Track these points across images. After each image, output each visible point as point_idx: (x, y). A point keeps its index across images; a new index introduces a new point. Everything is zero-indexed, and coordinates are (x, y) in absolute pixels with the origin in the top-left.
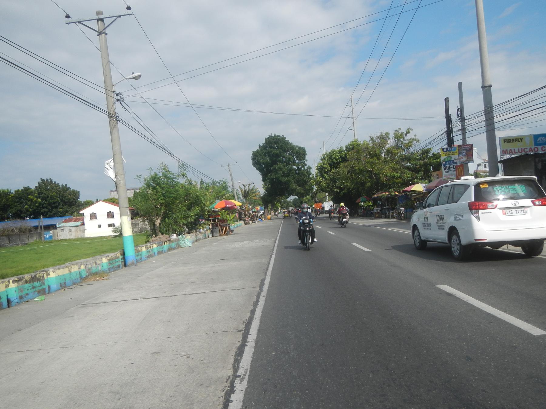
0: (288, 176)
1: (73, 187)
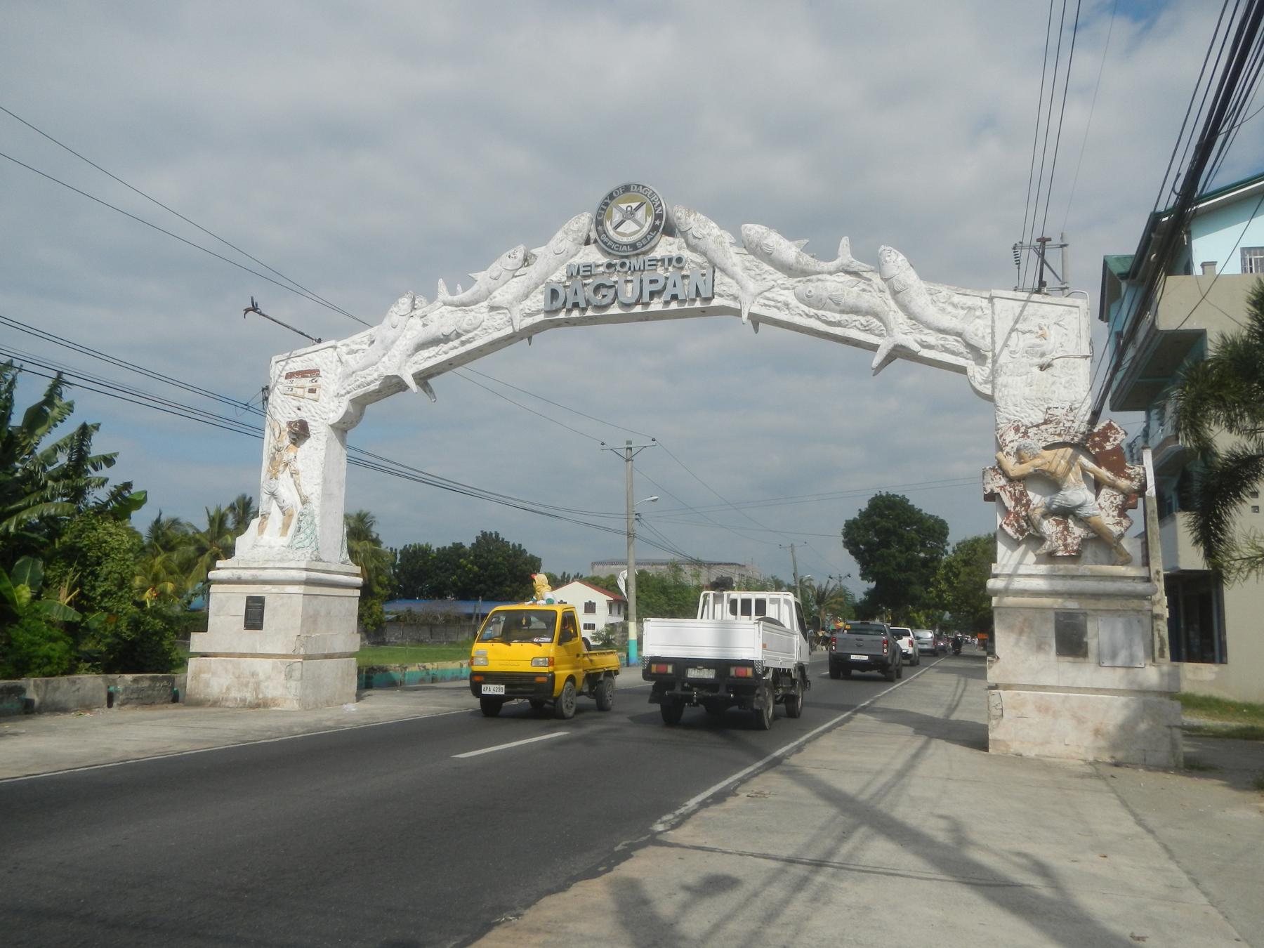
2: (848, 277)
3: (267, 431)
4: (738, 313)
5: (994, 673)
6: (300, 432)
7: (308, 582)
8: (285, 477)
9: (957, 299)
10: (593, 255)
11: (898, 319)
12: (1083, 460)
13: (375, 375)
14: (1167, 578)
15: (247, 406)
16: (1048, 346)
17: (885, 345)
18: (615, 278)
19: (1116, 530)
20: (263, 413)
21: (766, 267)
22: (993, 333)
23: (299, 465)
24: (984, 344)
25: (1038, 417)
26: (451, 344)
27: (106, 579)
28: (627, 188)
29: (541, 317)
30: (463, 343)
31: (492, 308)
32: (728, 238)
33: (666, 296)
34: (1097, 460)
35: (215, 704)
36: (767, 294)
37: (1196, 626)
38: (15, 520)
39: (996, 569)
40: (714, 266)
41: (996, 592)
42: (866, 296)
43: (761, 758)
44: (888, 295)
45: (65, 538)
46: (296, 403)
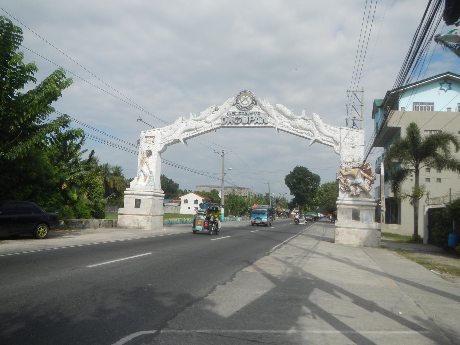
0: (306, 193)
1: (175, 181)
2: (304, 121)
3: (140, 153)
4: (275, 128)
5: (337, 224)
6: (149, 153)
7: (154, 195)
8: (145, 165)
9: (332, 128)
10: (235, 109)
11: (316, 132)
12: (362, 172)
13: (172, 138)
14: (386, 200)
15: (133, 145)
16: (354, 142)
17: (313, 139)
18: (241, 116)
19: (368, 189)
20: (137, 147)
21: (282, 116)
22: (341, 138)
23: (149, 163)
24: (338, 140)
25: (351, 160)
26: (194, 131)
27: (96, 193)
28: (245, 92)
29: (220, 125)
30: (197, 131)
31: (206, 122)
32: (272, 107)
33: (255, 122)
34: (365, 172)
35: (126, 228)
36: (283, 124)
37: (394, 214)
38: (73, 175)
39: (338, 198)
40: (268, 115)
41: (338, 204)
42: (309, 126)
43: (282, 242)
44: (314, 126)
45: (85, 181)
46: (148, 145)
